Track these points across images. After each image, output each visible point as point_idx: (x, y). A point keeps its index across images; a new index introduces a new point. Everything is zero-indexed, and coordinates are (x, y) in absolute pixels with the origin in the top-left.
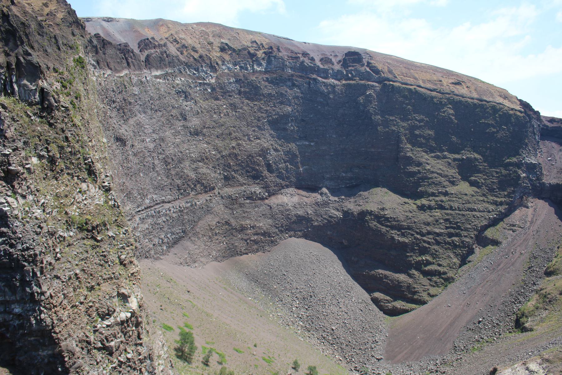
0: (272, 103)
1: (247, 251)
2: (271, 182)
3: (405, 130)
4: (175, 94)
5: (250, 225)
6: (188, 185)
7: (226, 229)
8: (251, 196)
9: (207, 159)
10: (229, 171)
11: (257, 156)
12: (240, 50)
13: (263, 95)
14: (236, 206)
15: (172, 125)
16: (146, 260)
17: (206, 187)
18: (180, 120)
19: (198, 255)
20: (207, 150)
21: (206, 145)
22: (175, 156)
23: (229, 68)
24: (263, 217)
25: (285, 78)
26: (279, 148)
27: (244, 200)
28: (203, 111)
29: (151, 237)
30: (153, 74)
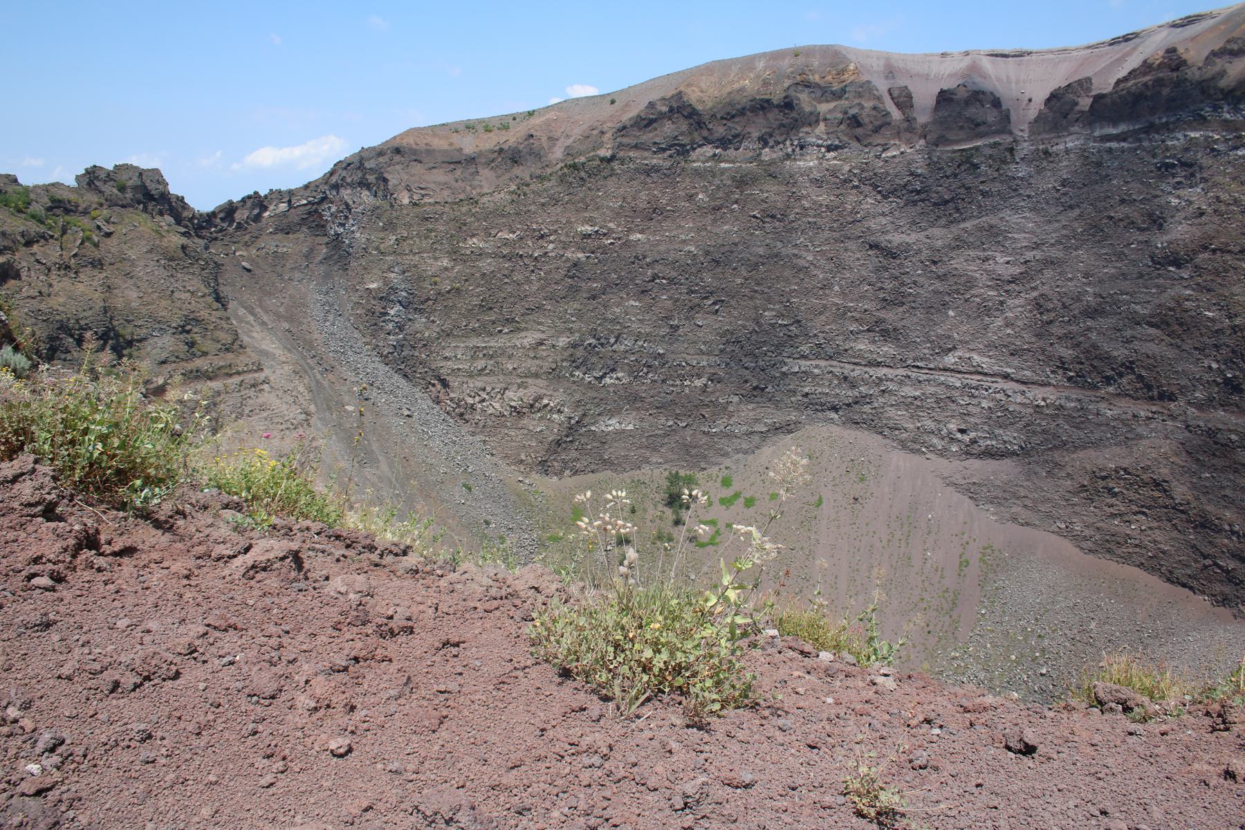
1: (1195, 584)
4: (1152, 172)
5: (1230, 525)
6: (1092, 365)
7: (1154, 499)
9: (1181, 325)
14: (1215, 461)
16: (880, 437)
17: (1149, 388)
18: (1141, 230)
19: (1018, 498)
22: (1078, 300)
29: (921, 414)
30: (1097, 134)
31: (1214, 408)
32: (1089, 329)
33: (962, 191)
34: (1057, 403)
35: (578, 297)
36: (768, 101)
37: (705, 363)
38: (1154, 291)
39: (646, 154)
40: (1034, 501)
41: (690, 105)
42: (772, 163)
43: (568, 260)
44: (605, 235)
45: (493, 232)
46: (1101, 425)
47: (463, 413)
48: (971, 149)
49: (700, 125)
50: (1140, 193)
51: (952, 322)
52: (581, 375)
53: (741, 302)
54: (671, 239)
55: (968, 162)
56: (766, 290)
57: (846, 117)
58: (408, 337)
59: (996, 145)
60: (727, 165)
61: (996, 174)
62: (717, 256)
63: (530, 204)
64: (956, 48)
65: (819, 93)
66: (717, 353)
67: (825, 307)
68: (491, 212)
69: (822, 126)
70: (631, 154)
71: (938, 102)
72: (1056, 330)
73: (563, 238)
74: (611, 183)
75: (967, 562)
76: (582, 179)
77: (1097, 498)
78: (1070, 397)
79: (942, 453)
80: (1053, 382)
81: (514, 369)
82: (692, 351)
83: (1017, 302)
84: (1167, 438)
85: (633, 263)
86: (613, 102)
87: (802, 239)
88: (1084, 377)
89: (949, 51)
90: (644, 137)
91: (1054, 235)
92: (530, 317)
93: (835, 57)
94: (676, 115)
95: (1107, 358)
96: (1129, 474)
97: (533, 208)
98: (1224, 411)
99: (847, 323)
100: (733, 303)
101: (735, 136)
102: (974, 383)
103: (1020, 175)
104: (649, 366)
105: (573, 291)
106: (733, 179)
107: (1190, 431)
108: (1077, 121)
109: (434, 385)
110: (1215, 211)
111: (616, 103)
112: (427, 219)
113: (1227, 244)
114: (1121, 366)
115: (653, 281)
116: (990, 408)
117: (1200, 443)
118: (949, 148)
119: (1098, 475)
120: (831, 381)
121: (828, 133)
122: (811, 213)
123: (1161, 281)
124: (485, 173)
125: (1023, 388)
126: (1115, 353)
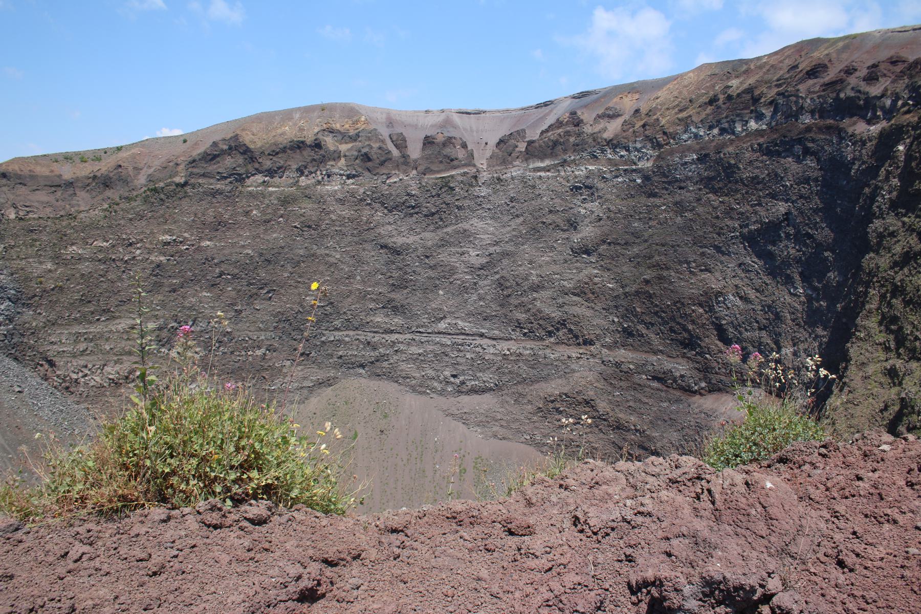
0: (754, 198)
2: (718, 363)
3: (891, 268)
5: (634, 426)
6: (538, 324)
8: (663, 376)
9: (593, 293)
10: (633, 322)
11: (694, 305)
12: (739, 95)
13: (741, 180)
14: (622, 384)
15: (542, 236)
16: (396, 384)
17: (577, 337)
19: (496, 421)
20: (596, 280)
21: (596, 271)
22: (526, 279)
23: (696, 136)
24: (669, 423)
25: (792, 140)
26: (752, 294)
27: (648, 379)
28: (612, 215)
29: (425, 366)
30: (531, 166)
31: (618, 348)
32: (535, 299)
33: (444, 206)
34: (517, 352)
35: (161, 291)
36: (303, 142)
37: (263, 337)
38: (574, 271)
39: (212, 181)
40: (508, 422)
41: (245, 145)
42: (307, 187)
43: (152, 262)
44: (181, 242)
45: (90, 241)
46: (548, 365)
47: (68, 387)
48: (449, 176)
49: (252, 159)
50: (562, 206)
51: (441, 299)
52: (167, 351)
53: (289, 291)
54: (233, 245)
55: (446, 185)
56: (307, 281)
57: (360, 154)
58: (18, 327)
59: (465, 174)
60: (274, 189)
61: (466, 194)
62: (268, 257)
63: (120, 219)
64: (435, 107)
65: (340, 137)
66: (272, 329)
67: (350, 292)
68: (87, 226)
69: (343, 161)
70: (200, 181)
71: (424, 144)
72: (514, 301)
73: (147, 246)
74: (185, 203)
75: (465, 470)
76: (162, 199)
77: (549, 416)
78: (527, 347)
79: (442, 393)
80: (514, 337)
81: (111, 349)
82: (252, 329)
83: (485, 282)
84: (591, 370)
85: (204, 263)
86: (185, 141)
87: (331, 243)
88: (534, 332)
89: (430, 109)
90: (210, 168)
91: (507, 235)
92: (123, 307)
93: (351, 112)
94: (234, 152)
95: (548, 318)
96: (569, 397)
97: (122, 222)
98: (625, 349)
99: (367, 303)
100: (282, 291)
101: (279, 168)
102: (460, 341)
103: (482, 194)
104: (220, 342)
105: (158, 286)
106: (279, 199)
107: (605, 365)
108: (518, 157)
109: (42, 365)
110: (608, 217)
111: (188, 142)
112: (32, 231)
113: (617, 239)
114: (557, 324)
115: (220, 277)
116: (472, 358)
117: (612, 372)
118: (433, 176)
119: (548, 399)
120: (358, 346)
121: (347, 166)
122: (337, 223)
123: (578, 264)
124: (82, 194)
125: (494, 342)
126: (553, 315)
